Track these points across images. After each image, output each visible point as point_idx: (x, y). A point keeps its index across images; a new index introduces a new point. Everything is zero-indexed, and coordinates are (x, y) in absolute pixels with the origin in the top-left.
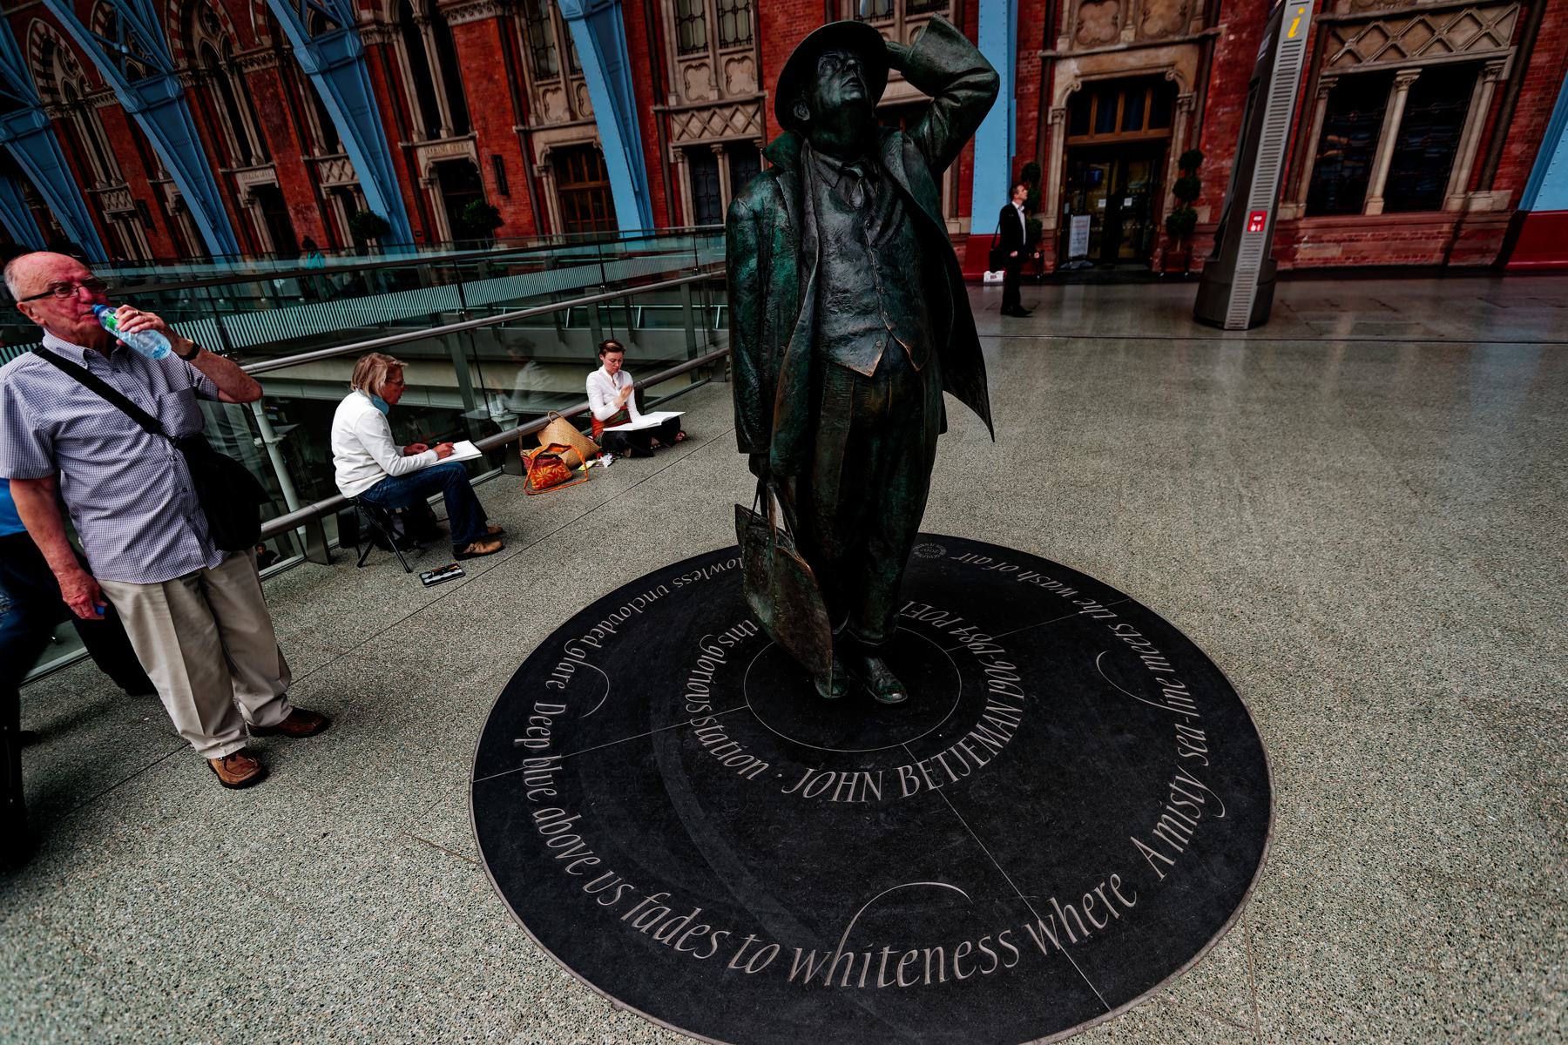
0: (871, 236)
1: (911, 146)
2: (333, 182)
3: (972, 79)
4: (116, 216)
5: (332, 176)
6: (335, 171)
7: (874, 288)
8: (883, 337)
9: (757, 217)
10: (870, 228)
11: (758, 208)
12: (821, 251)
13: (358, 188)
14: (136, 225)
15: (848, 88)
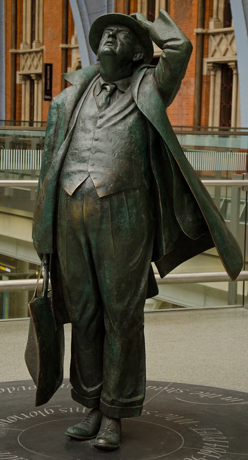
0: (100, 122)
1: (150, 78)
2: (218, 58)
3: (169, 44)
4: (27, 77)
5: (218, 52)
6: (223, 47)
7: (89, 149)
8: (86, 176)
9: (58, 107)
10: (101, 117)
11: (60, 103)
12: (74, 128)
13: (236, 62)
14: (39, 88)
15: (106, 46)
